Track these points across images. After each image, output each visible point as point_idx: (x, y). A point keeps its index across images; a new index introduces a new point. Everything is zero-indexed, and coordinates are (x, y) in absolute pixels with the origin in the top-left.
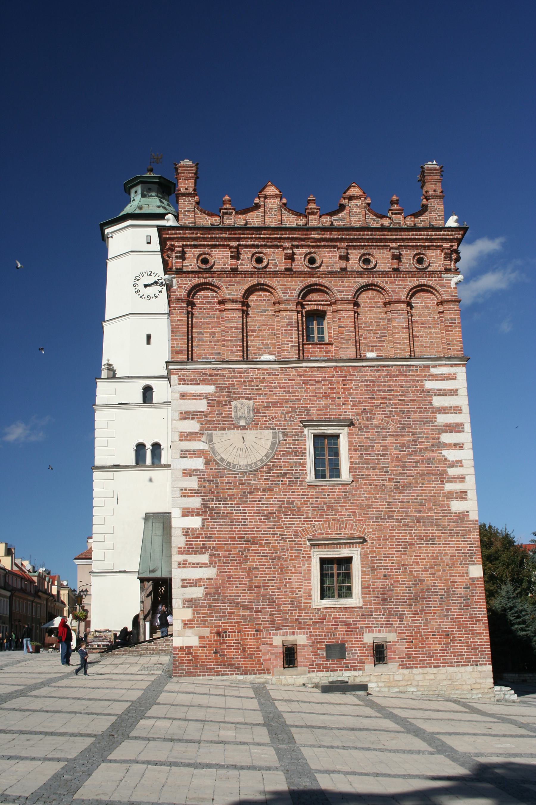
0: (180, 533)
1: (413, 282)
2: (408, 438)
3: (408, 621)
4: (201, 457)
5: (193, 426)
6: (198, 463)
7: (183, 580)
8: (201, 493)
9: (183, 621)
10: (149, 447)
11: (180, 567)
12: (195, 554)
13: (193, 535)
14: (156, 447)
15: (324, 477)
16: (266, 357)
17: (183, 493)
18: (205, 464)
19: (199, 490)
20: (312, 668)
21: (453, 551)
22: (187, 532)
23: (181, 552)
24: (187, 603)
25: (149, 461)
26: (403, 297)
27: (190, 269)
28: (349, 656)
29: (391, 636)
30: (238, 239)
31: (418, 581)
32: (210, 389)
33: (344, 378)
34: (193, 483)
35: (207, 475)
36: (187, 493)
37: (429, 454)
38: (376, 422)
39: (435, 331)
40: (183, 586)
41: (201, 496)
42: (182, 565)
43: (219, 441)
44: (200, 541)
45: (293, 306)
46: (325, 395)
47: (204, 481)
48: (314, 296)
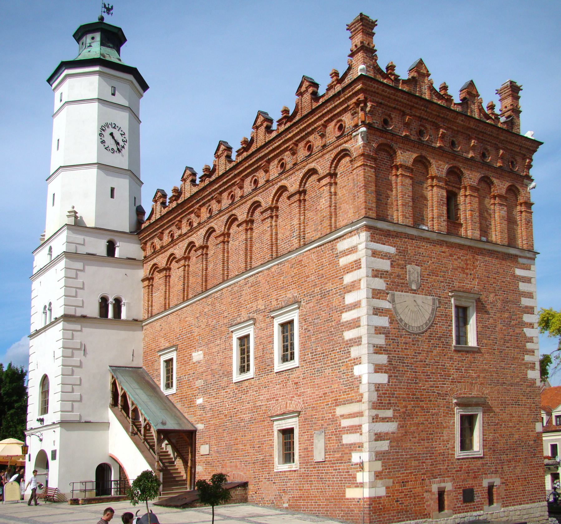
0: (373, 388)
4: (387, 316)
6: (384, 321)
7: (376, 434)
8: (387, 351)
9: (375, 472)
11: (373, 422)
12: (384, 409)
13: (382, 391)
17: (375, 350)
18: (390, 323)
19: (385, 348)
22: (378, 387)
34: (381, 340)
35: (392, 334)
40: (376, 440)
41: (388, 353)
42: (375, 420)
43: (399, 302)
44: (387, 397)
47: (390, 339)
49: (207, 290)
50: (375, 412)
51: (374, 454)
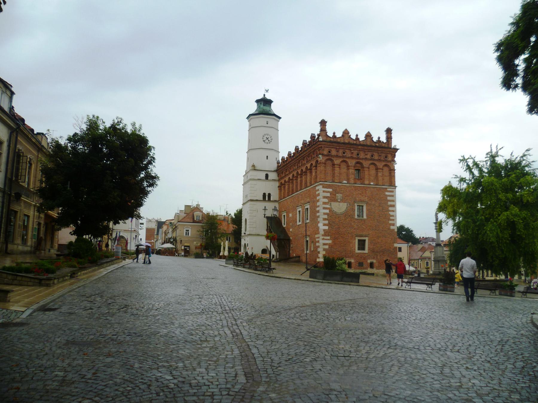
1: (384, 163)
2: (381, 208)
3: (379, 257)
5: (326, 200)
6: (327, 211)
10: (267, 194)
14: (269, 195)
15: (359, 217)
16: (345, 182)
20: (355, 269)
21: (390, 240)
23: (323, 235)
24: (324, 250)
25: (267, 199)
26: (381, 167)
27: (325, 154)
28: (364, 266)
29: (374, 261)
30: (339, 146)
31: (381, 247)
32: (331, 190)
33: (365, 190)
34: (326, 217)
36: (325, 219)
37: (386, 213)
38: (373, 202)
39: (388, 178)
45: (353, 168)
46: (360, 194)
48: (358, 165)
49: (293, 193)
50: (323, 237)
51: (322, 249)
